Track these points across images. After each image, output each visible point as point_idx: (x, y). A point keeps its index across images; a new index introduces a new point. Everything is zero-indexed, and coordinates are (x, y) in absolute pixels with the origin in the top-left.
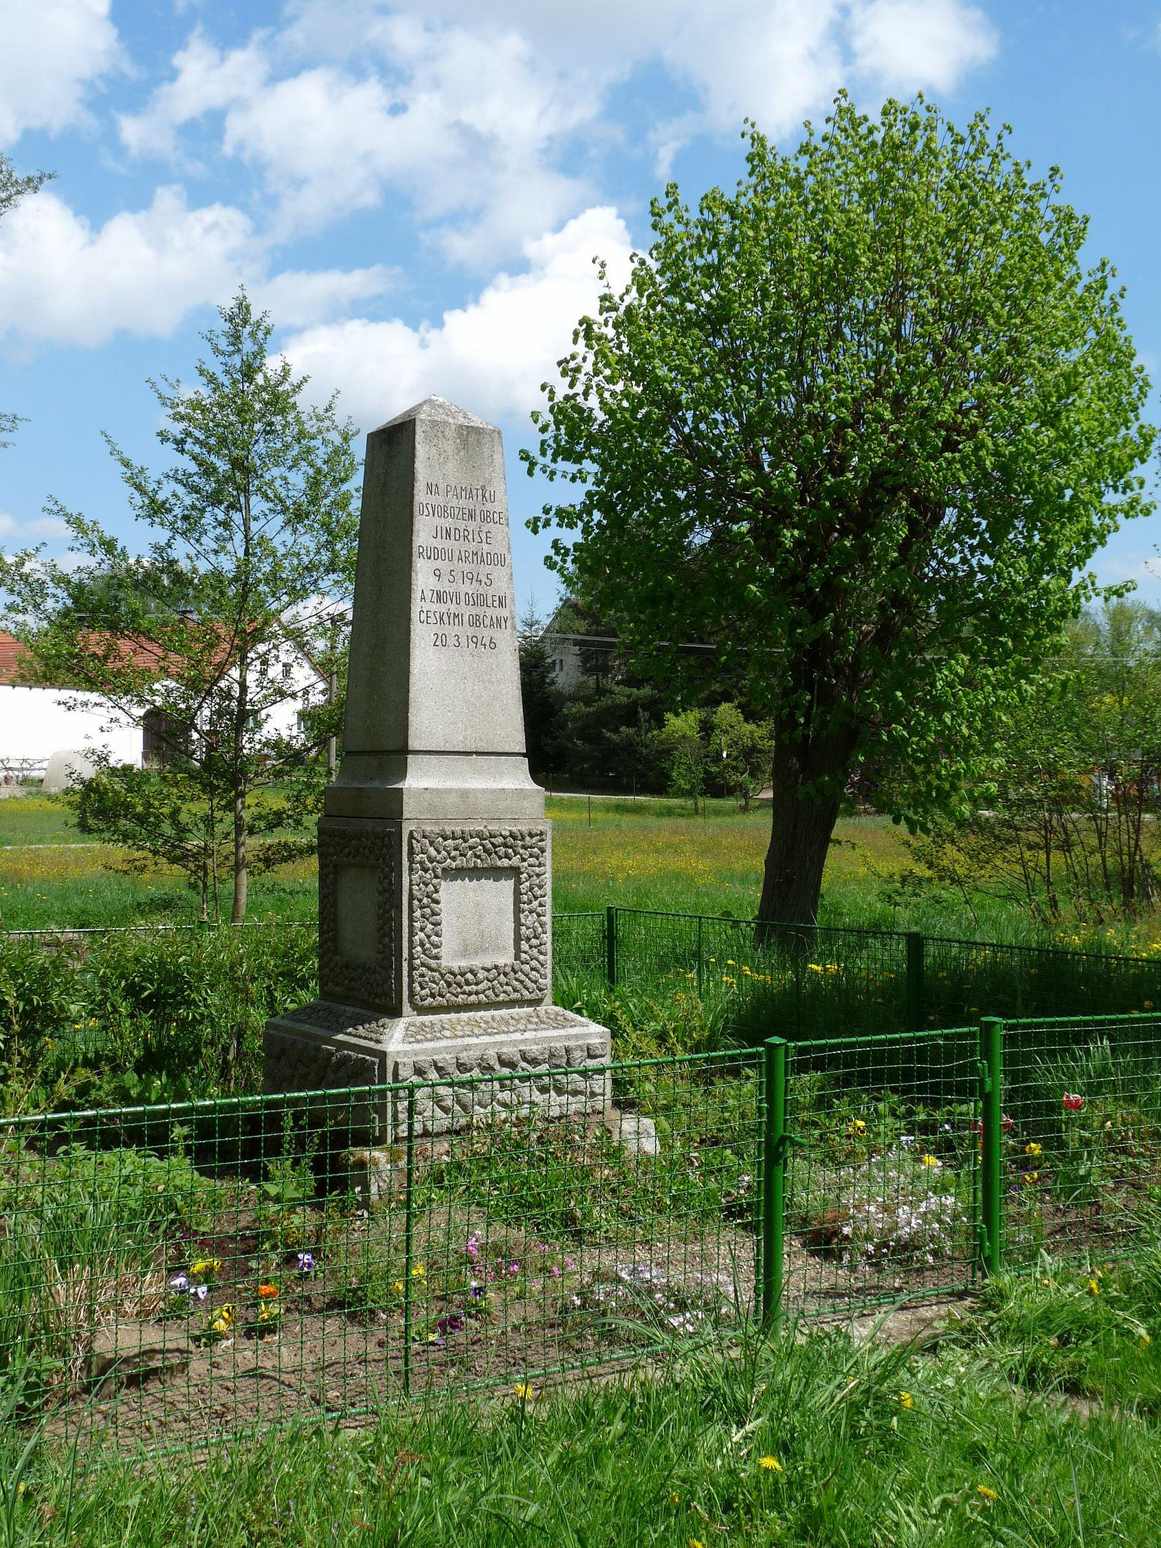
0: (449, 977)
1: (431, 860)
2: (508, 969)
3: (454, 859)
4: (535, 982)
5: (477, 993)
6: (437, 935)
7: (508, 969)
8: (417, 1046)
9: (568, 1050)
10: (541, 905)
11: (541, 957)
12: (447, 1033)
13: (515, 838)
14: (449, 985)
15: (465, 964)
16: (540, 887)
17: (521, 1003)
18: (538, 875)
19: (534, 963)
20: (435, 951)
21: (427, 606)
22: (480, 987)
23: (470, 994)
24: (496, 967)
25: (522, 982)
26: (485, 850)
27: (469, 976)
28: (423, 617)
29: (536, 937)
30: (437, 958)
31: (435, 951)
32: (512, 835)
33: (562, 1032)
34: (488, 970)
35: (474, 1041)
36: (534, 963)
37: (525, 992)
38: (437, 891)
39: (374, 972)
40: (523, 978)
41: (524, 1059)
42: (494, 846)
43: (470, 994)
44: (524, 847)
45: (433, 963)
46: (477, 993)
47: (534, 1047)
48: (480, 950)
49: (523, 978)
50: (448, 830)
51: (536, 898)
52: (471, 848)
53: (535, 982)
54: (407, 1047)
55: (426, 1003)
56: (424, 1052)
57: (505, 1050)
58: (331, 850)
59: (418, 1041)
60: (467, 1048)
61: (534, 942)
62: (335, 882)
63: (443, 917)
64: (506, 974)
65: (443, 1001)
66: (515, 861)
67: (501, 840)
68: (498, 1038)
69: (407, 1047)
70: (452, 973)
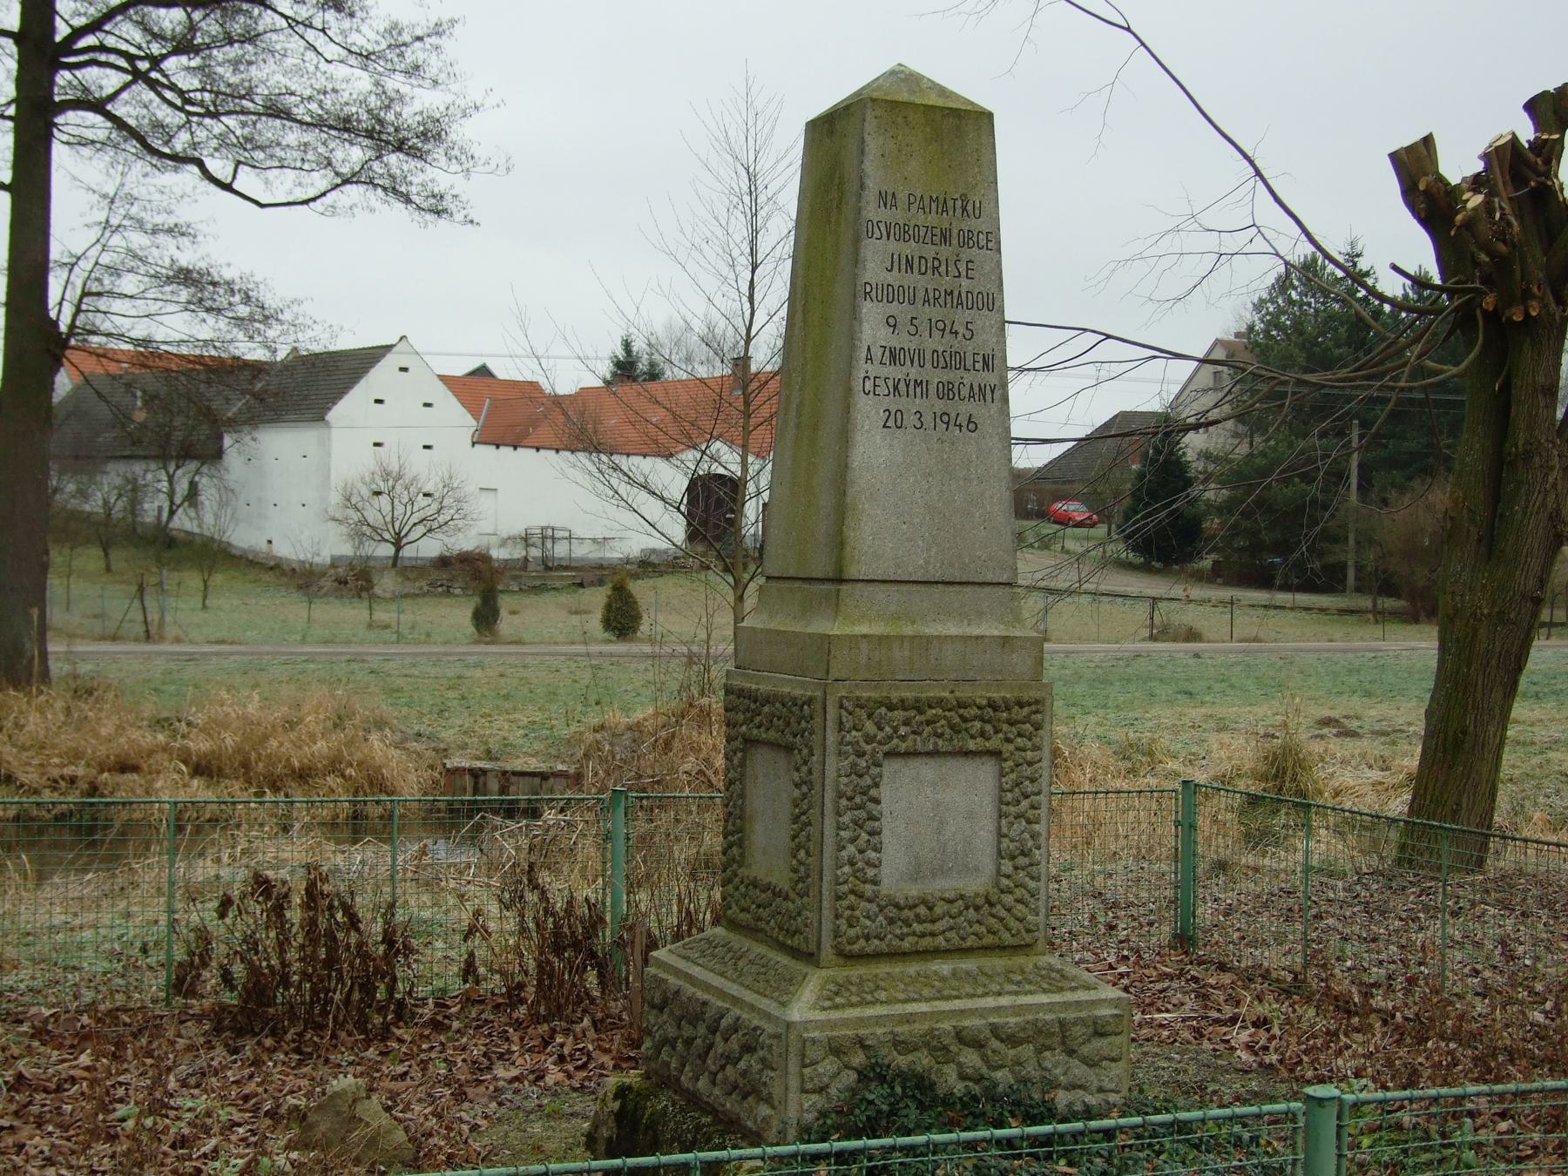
0: (892, 912)
1: (869, 739)
2: (980, 901)
3: (903, 738)
4: (1021, 920)
5: (933, 935)
6: (877, 850)
7: (980, 901)
8: (835, 1015)
9: (804, 1091)
10: (1033, 807)
11: (1032, 884)
12: (883, 995)
13: (995, 708)
14: (891, 921)
15: (914, 891)
16: (1033, 780)
17: (1002, 948)
18: (1030, 764)
19: (1019, 892)
20: (871, 872)
21: (873, 369)
22: (939, 926)
23: (923, 935)
24: (962, 897)
25: (1002, 920)
26: (952, 727)
27: (922, 910)
28: (869, 385)
29: (1023, 853)
30: (875, 882)
31: (871, 872)
32: (992, 705)
33: (1056, 998)
34: (951, 902)
35: (923, 1007)
36: (1019, 892)
37: (1006, 936)
38: (877, 785)
39: (786, 898)
40: (1003, 913)
41: (997, 1037)
42: (965, 720)
43: (923, 935)
44: (1011, 723)
45: (868, 889)
46: (933, 935)
47: (1012, 1020)
48: (941, 871)
49: (1003, 913)
50: (895, 696)
51: (1026, 797)
52: (928, 723)
53: (1021, 920)
54: (820, 1016)
55: (856, 947)
56: (845, 1023)
57: (967, 1023)
58: (741, 717)
59: (836, 1007)
60: (909, 1019)
61: (1022, 861)
62: (742, 764)
63: (886, 824)
64: (977, 908)
65: (881, 946)
66: (994, 743)
67: (974, 711)
68: (957, 1004)
69: (820, 1016)
70: (897, 906)
